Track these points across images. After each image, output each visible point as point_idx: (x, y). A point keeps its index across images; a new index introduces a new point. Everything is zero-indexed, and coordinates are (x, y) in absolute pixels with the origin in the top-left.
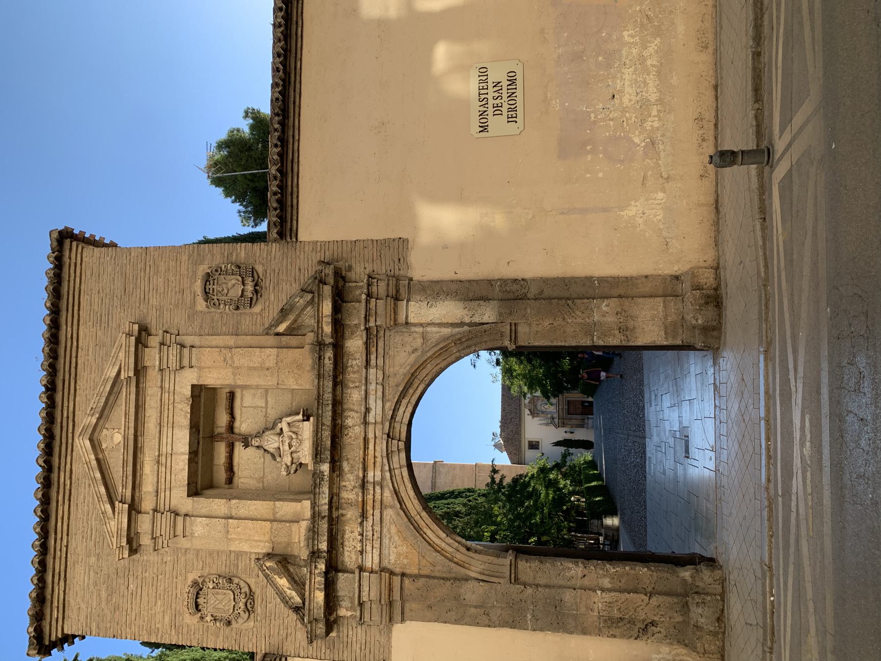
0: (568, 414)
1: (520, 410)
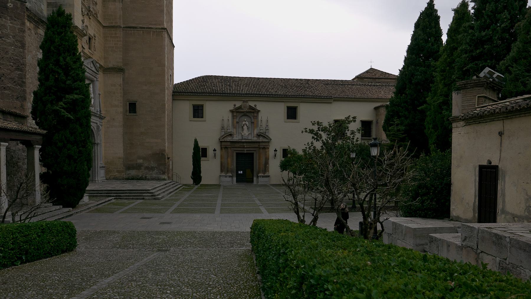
0: (237, 153)
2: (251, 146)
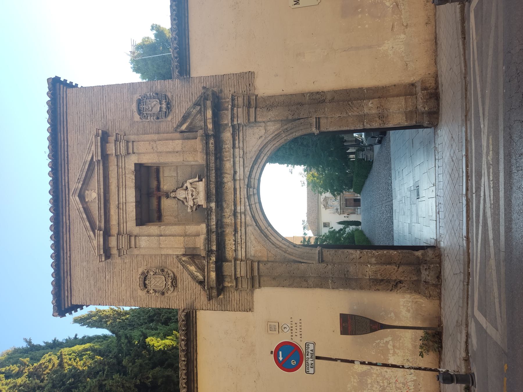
1: (318, 205)
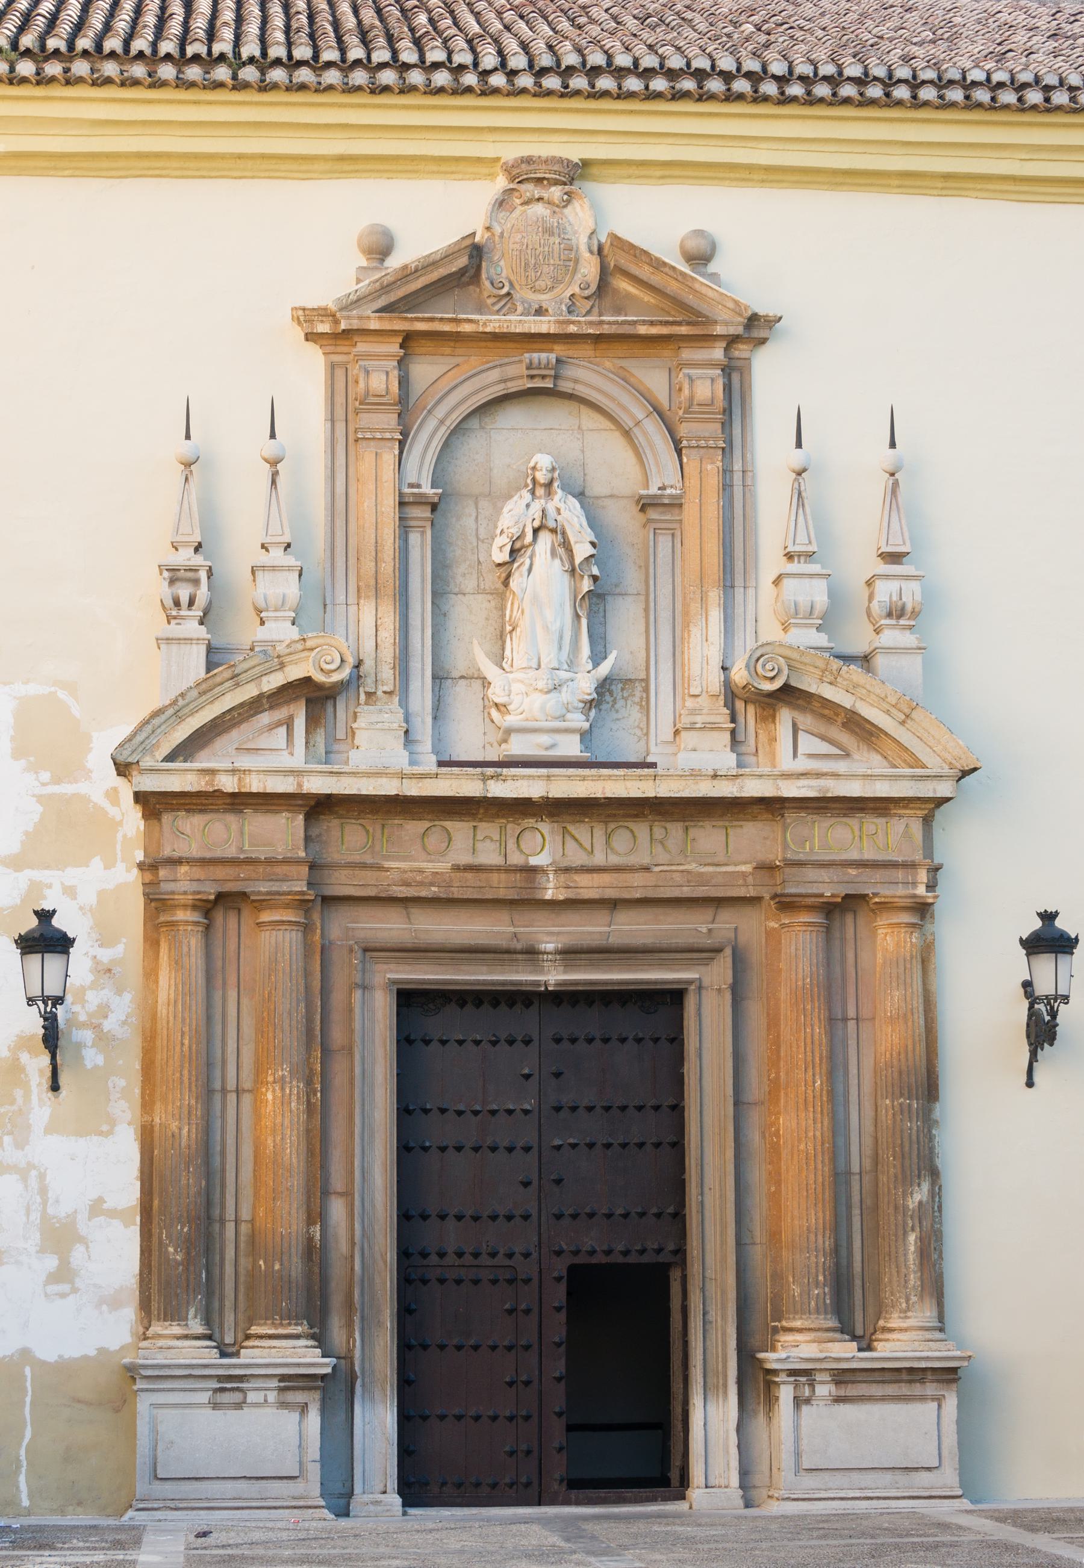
2: (637, 885)
